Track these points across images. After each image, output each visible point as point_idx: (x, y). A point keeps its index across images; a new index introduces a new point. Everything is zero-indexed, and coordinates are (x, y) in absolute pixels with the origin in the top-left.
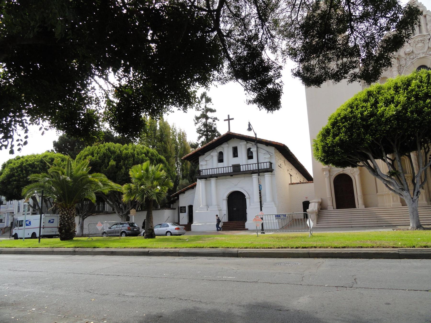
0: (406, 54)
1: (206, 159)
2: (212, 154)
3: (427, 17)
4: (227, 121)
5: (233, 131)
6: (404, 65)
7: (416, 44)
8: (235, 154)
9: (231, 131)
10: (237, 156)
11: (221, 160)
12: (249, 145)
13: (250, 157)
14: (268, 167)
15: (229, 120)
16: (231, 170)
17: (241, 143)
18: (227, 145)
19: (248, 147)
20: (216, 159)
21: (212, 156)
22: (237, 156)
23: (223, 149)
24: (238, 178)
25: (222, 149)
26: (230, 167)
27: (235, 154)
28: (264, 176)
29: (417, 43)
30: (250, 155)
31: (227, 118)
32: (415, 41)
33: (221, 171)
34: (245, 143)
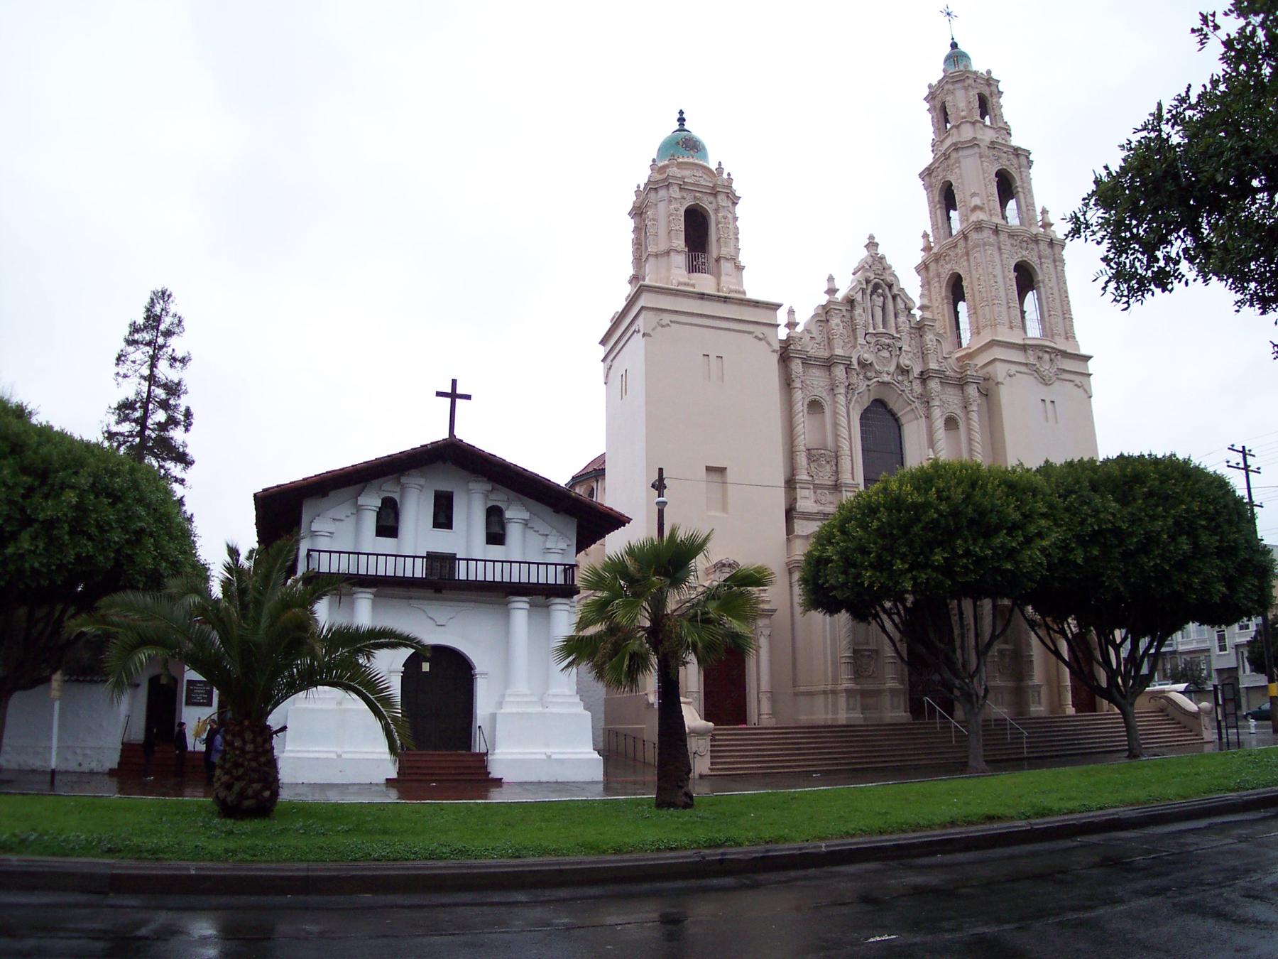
0: (859, 364)
1: (332, 513)
2: (361, 501)
3: (899, 299)
4: (448, 400)
5: (468, 434)
6: (854, 387)
7: (879, 350)
8: (443, 519)
9: (459, 434)
10: (449, 525)
11: (388, 528)
12: (498, 499)
13: (496, 537)
14: (560, 581)
15: (453, 396)
16: (418, 570)
17: (471, 486)
18: (422, 481)
19: (490, 504)
20: (370, 521)
21: (359, 509)
22: (449, 525)
23: (403, 489)
24: (393, 597)
25: (398, 489)
26: (423, 557)
27: (443, 519)
28: (548, 606)
29: (881, 348)
30: (496, 529)
31: (449, 390)
32: (879, 342)
33: (385, 568)
34: (489, 487)
